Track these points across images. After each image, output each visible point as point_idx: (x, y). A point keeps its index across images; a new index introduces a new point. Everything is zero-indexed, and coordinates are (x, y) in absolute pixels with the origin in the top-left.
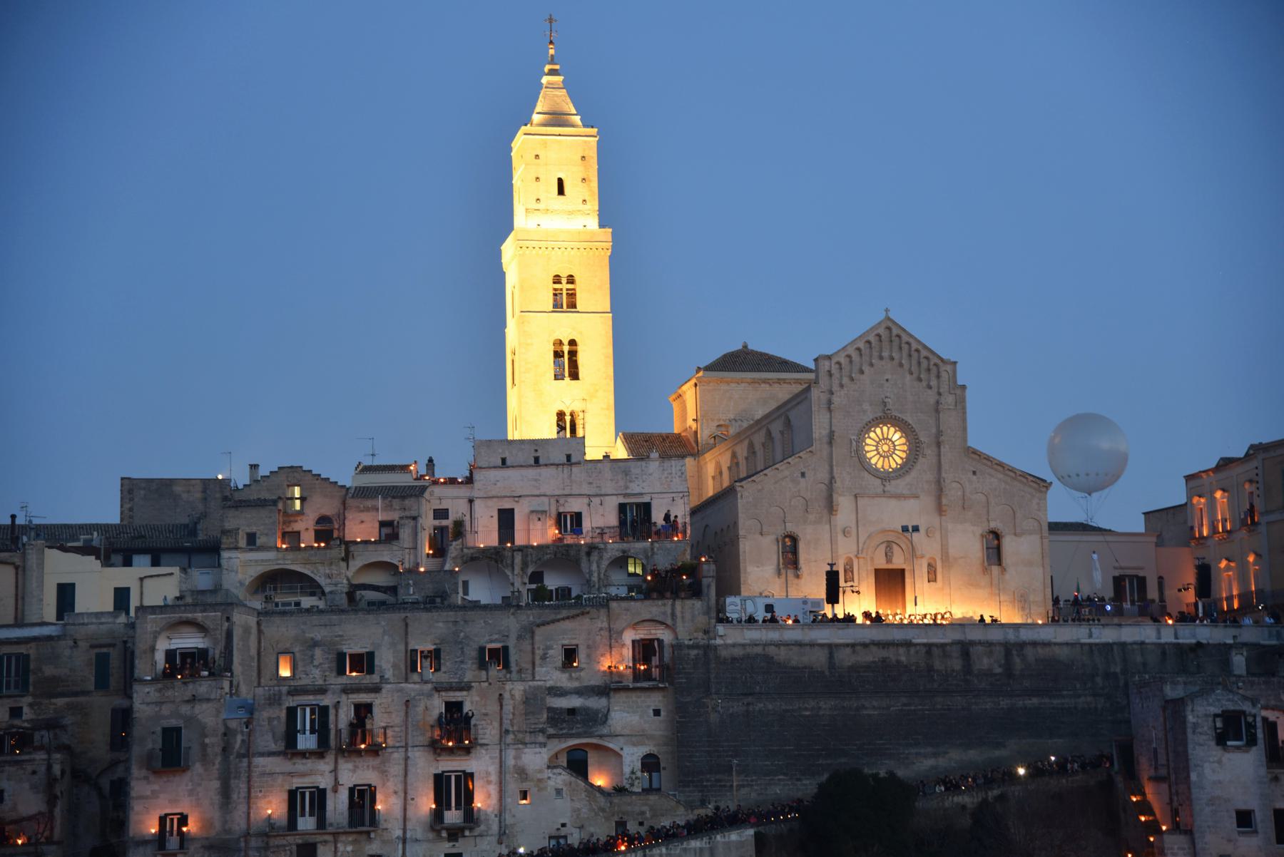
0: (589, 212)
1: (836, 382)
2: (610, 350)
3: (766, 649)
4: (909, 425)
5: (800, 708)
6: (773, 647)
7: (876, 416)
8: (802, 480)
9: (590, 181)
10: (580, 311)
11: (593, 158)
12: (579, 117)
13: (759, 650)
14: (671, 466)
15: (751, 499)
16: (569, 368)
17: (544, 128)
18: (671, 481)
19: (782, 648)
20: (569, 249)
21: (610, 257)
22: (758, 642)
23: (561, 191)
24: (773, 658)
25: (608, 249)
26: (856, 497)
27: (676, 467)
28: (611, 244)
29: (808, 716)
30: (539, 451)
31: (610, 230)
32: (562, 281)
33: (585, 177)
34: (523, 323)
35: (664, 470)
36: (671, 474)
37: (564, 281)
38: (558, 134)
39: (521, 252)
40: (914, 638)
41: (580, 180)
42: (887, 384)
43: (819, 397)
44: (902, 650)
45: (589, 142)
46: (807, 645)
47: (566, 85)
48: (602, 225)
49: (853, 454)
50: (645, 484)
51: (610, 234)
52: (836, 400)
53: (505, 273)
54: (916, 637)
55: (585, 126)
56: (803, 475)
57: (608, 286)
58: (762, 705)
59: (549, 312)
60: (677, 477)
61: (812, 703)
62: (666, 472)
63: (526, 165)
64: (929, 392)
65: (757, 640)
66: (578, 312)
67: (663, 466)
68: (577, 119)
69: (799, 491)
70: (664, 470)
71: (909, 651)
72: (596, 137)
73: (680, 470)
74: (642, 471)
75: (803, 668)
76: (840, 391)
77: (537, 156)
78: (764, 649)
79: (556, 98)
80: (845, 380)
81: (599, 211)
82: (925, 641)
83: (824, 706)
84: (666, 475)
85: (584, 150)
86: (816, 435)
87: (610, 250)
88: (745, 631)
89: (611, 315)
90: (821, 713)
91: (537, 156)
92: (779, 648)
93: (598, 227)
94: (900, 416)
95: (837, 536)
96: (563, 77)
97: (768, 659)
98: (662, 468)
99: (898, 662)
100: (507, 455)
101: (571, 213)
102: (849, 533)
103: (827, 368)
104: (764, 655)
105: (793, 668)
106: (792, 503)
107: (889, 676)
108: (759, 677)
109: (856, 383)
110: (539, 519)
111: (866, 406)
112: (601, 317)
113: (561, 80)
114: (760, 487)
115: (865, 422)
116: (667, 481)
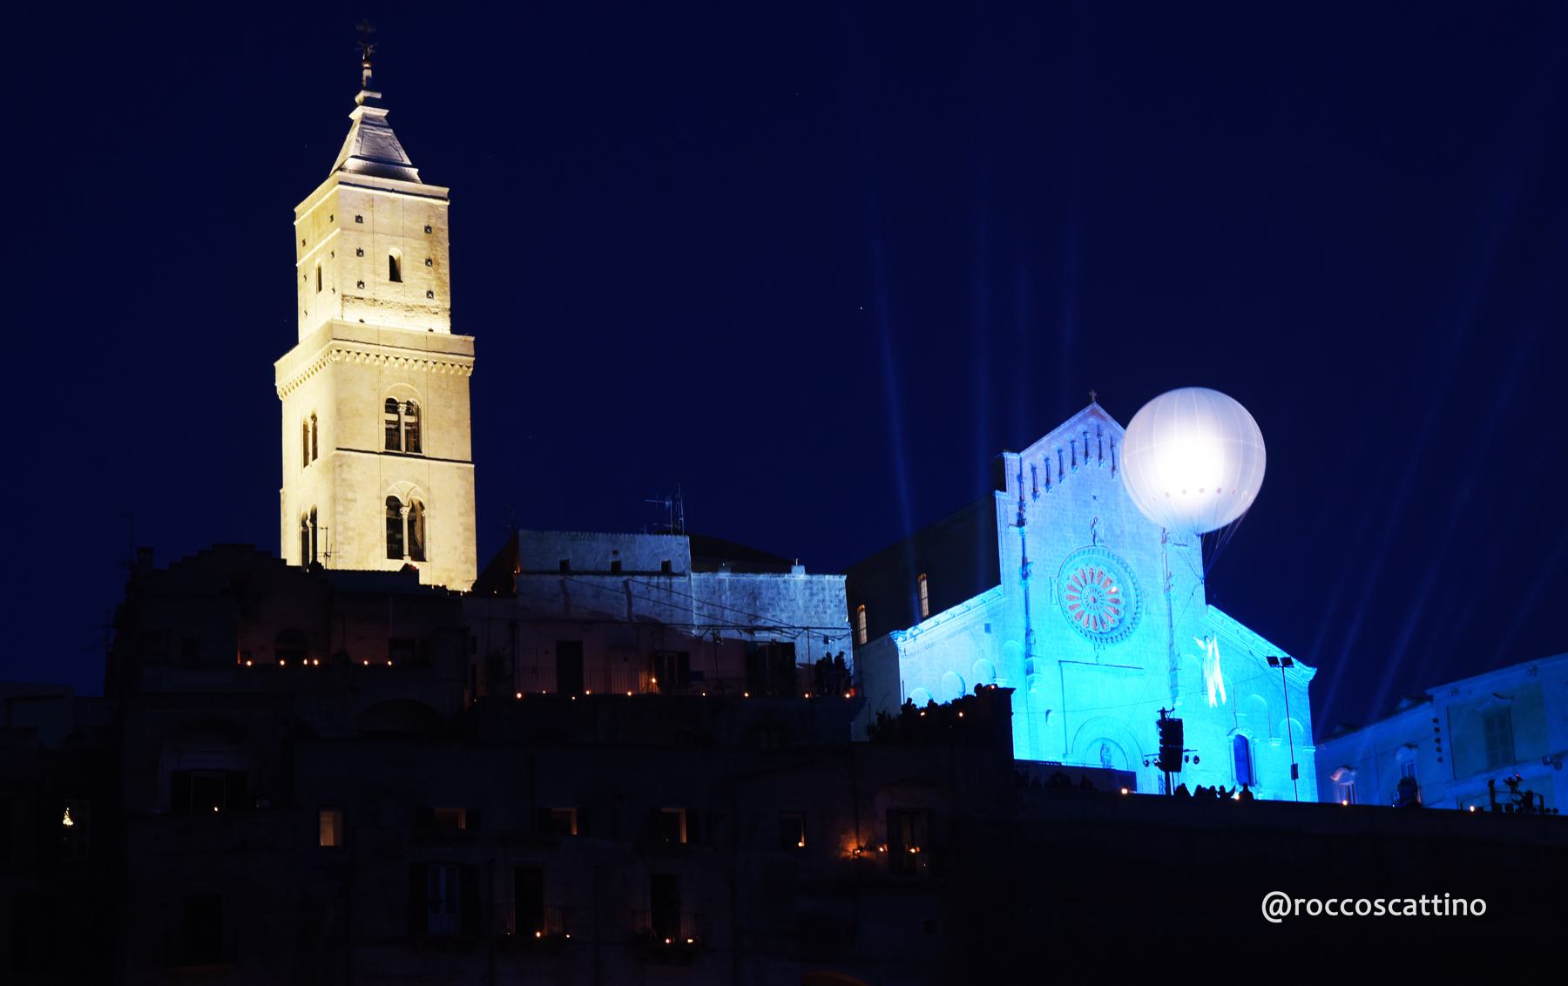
0: (437, 310)
2: (472, 520)
9: (438, 264)
10: (427, 456)
11: (442, 230)
12: (417, 170)
16: (409, 545)
17: (370, 178)
20: (411, 361)
21: (470, 378)
23: (395, 275)
25: (468, 367)
27: (830, 590)
28: (474, 359)
30: (622, 554)
31: (472, 339)
32: (400, 410)
33: (432, 257)
34: (341, 466)
37: (402, 409)
38: (390, 189)
39: (338, 359)
41: (424, 261)
45: (437, 207)
47: (391, 121)
48: (455, 329)
51: (472, 345)
53: (280, 403)
55: (425, 181)
57: (468, 422)
59: (380, 454)
63: (343, 229)
66: (424, 457)
67: (811, 589)
68: (414, 172)
70: (812, 594)
72: (446, 200)
77: (359, 219)
79: (379, 140)
81: (451, 309)
85: (429, 217)
87: (471, 369)
89: (473, 466)
91: (359, 219)
93: (449, 332)
96: (387, 111)
100: (570, 557)
101: (409, 308)
110: (626, 659)
112: (458, 468)
113: (384, 114)
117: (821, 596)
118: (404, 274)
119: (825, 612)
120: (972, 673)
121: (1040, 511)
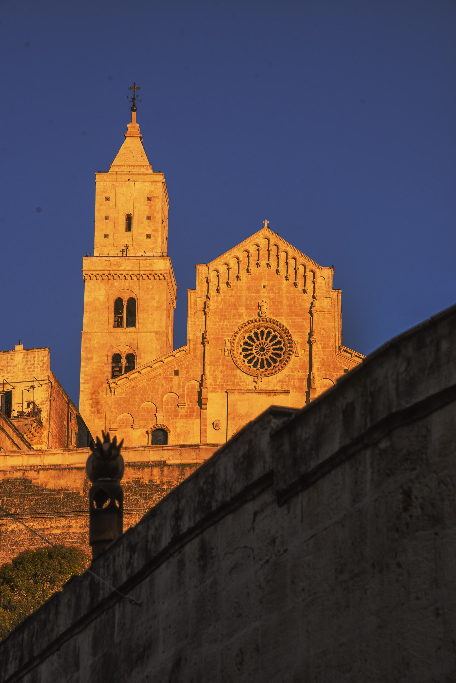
1: (213, 288)
3: (26, 474)
4: (284, 326)
5: (51, 527)
6: (33, 472)
7: (251, 318)
8: (175, 378)
13: (18, 475)
14: (35, 357)
15: (124, 396)
18: (34, 371)
19: (41, 472)
22: (18, 468)
23: (129, 227)
24: (32, 481)
26: (227, 392)
27: (38, 358)
29: (57, 535)
35: (27, 361)
36: (34, 364)
40: (169, 459)
42: (263, 290)
43: (196, 302)
44: (156, 471)
46: (65, 469)
49: (227, 354)
50: (9, 375)
52: (212, 305)
54: (171, 458)
56: (176, 373)
58: (15, 525)
60: (39, 367)
61: (64, 523)
62: (29, 363)
64: (305, 296)
65: (16, 466)
67: (27, 358)
69: (171, 388)
70: (27, 361)
71: (162, 471)
73: (42, 360)
74: (8, 363)
75: (59, 490)
76: (217, 296)
78: (24, 474)
80: (223, 286)
82: (178, 462)
83: (75, 525)
84: (28, 366)
86: (190, 336)
88: (8, 457)
90: (71, 531)
92: (38, 472)
94: (274, 318)
95: (206, 429)
97: (26, 482)
98: (25, 360)
99: (151, 481)
102: (217, 425)
103: (205, 275)
104: (24, 479)
105: (50, 490)
106: (164, 398)
107: (140, 495)
108: (16, 500)
109: (233, 290)
111: (242, 310)
114: (133, 384)
115: (240, 325)
116: (29, 371)
117: (32, 362)
118: (135, 225)
119: (34, 371)
120: (162, 401)
121: (222, 299)
